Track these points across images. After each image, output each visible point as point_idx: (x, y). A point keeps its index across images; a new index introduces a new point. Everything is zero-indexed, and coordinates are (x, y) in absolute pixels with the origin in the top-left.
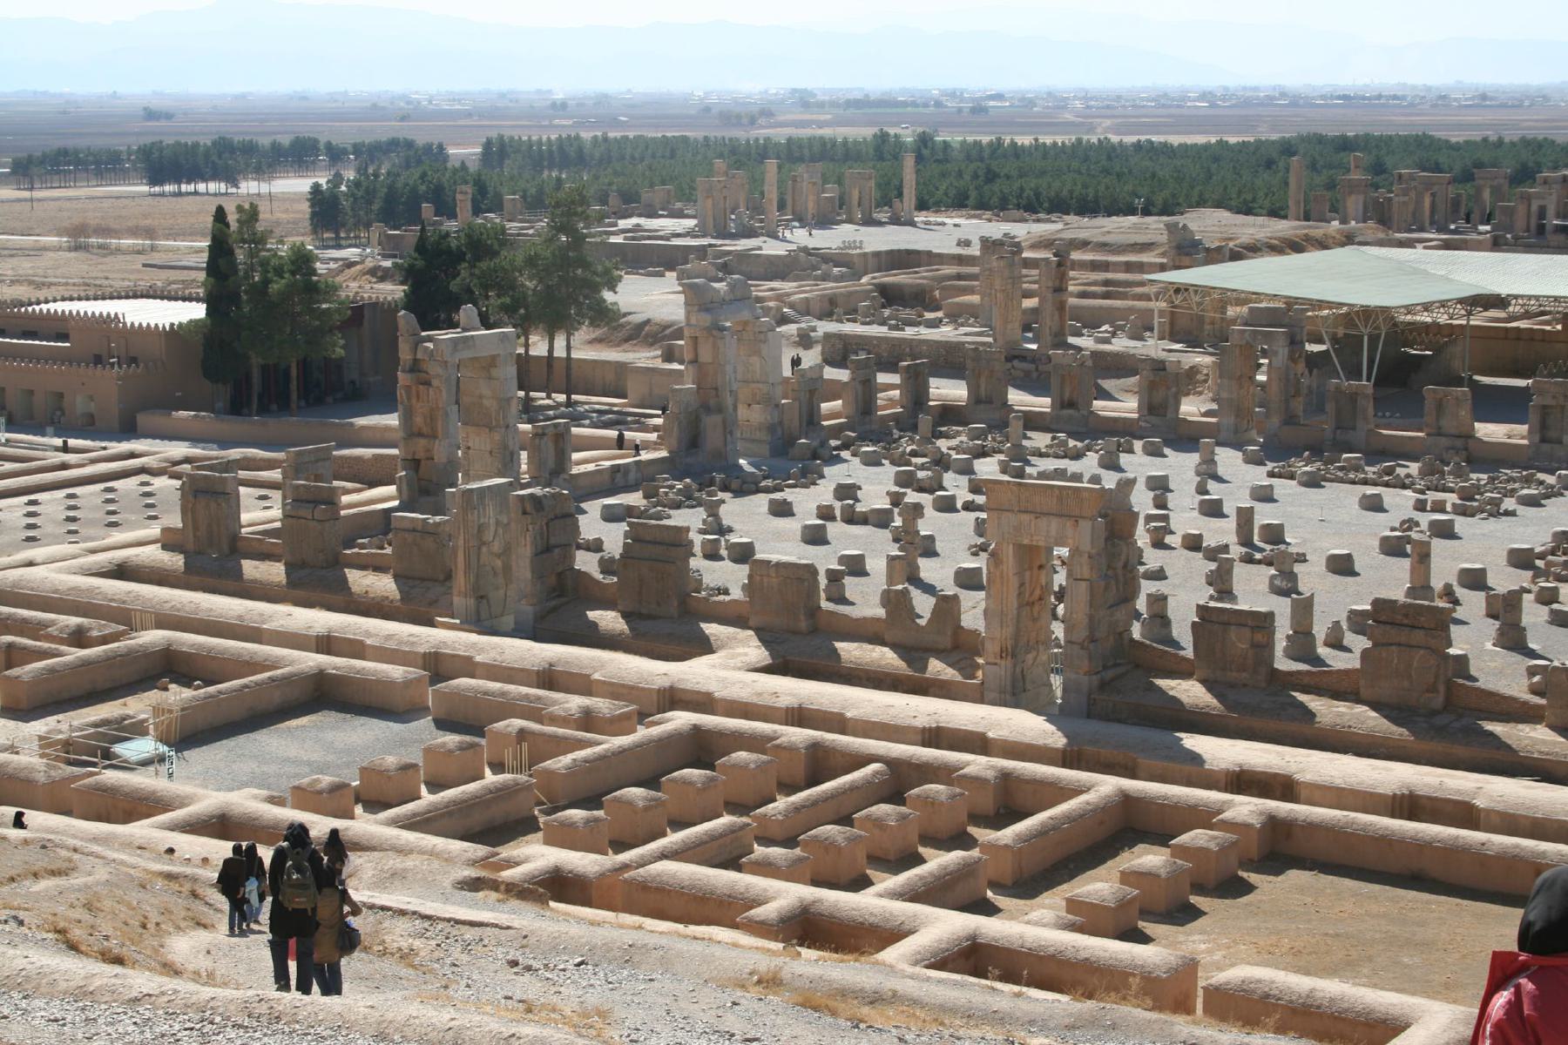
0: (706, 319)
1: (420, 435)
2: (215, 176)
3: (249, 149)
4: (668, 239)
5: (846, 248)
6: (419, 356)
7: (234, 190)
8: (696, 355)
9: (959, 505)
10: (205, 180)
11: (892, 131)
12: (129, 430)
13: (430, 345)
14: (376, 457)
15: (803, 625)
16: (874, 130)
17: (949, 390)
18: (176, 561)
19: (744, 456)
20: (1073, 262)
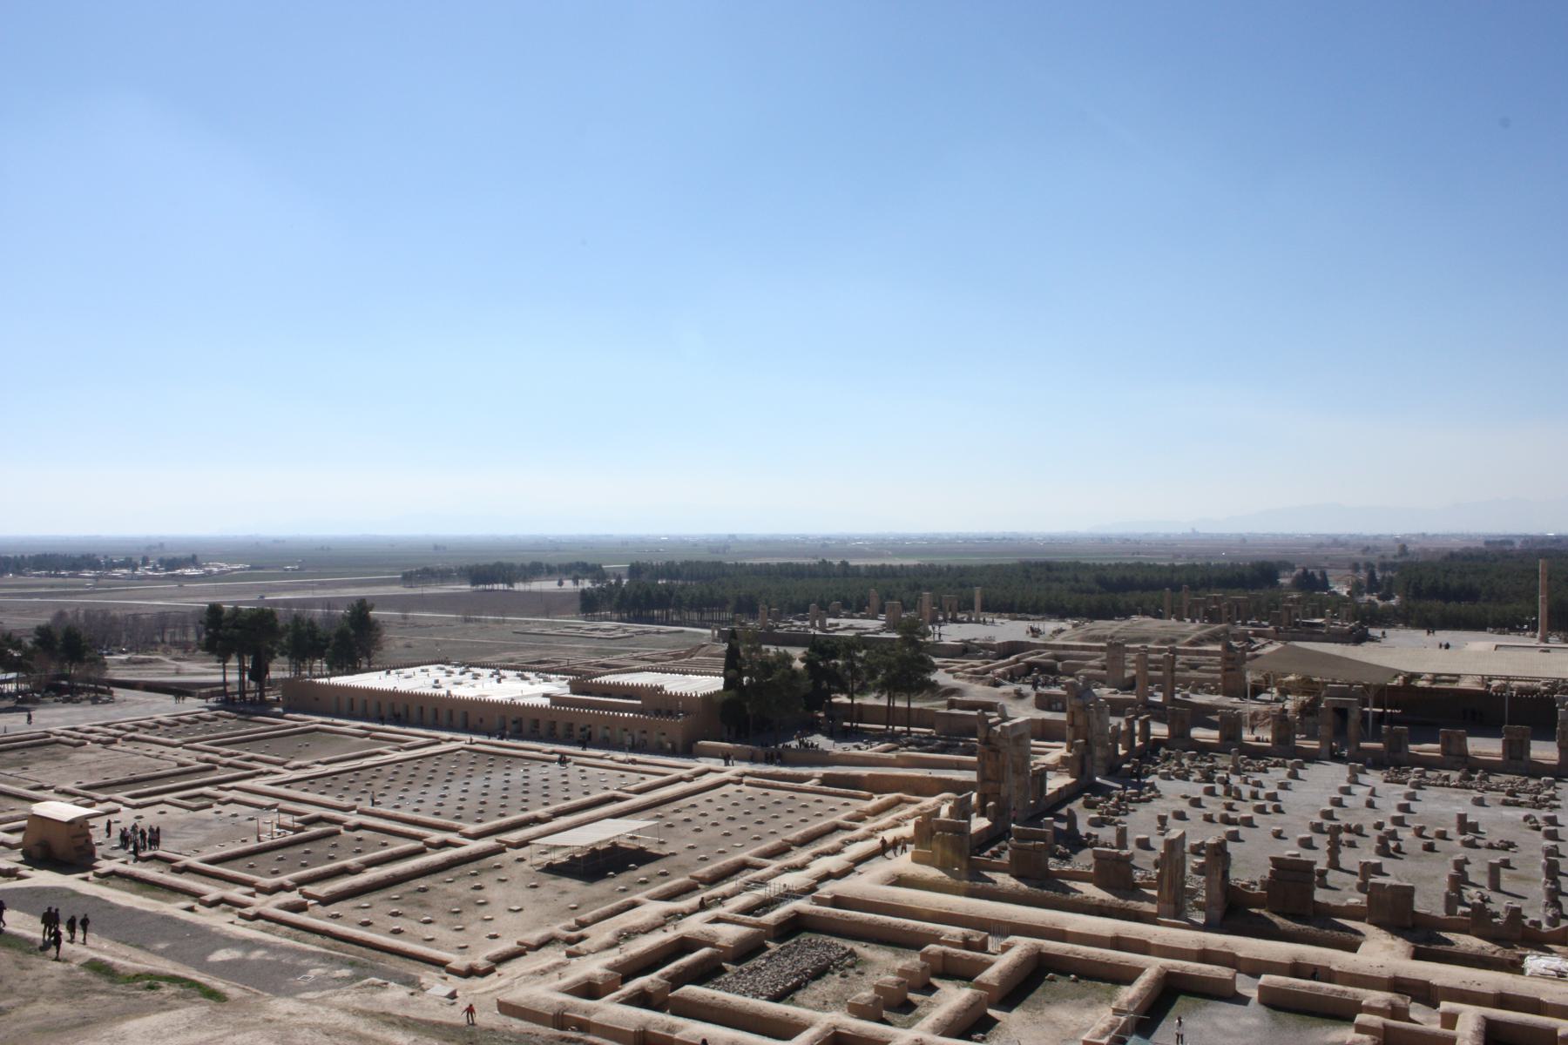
0: (1078, 702)
1: (989, 780)
2: (503, 582)
3: (511, 567)
4: (878, 634)
5: (987, 640)
6: (991, 735)
7: (511, 588)
8: (1073, 721)
9: (1269, 809)
10: (497, 582)
11: (828, 560)
12: (689, 751)
13: (998, 729)
14: (870, 775)
15: (1410, 923)
16: (820, 560)
17: (1159, 730)
18: (932, 873)
19: (1098, 775)
20: (1219, 665)
